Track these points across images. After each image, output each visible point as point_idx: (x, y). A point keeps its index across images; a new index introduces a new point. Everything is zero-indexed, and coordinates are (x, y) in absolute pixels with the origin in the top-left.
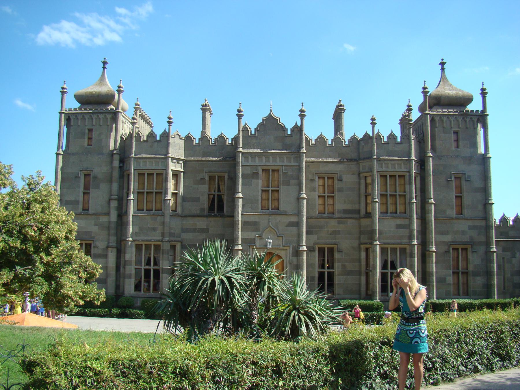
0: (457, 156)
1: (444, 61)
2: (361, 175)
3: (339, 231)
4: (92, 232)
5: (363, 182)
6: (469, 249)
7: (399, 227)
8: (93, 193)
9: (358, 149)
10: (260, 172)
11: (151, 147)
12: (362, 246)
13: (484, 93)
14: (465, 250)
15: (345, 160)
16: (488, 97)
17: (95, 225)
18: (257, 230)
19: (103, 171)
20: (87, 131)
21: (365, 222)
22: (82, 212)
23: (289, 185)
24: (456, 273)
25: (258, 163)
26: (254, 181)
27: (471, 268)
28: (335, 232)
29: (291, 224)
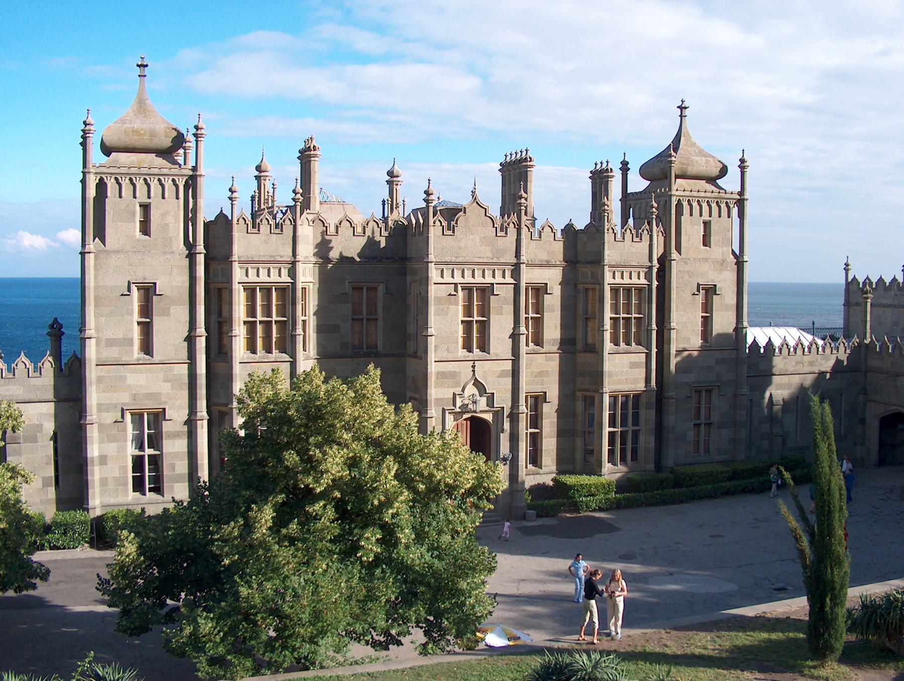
0: (707, 260)
1: (686, 104)
2: (580, 287)
3: (547, 372)
4: (160, 394)
5: (581, 296)
6: (715, 392)
7: (633, 365)
8: (159, 324)
9: (575, 244)
10: (460, 294)
11: (266, 242)
12: (579, 394)
13: (742, 165)
14: (709, 391)
15: (558, 263)
16: (748, 171)
17: (166, 381)
18: (456, 385)
19: (174, 284)
20: (138, 208)
21: (583, 358)
22: (138, 360)
23: (502, 314)
24: (697, 425)
25: (458, 279)
26: (452, 307)
27: (715, 417)
28: (541, 374)
29: (502, 374)
